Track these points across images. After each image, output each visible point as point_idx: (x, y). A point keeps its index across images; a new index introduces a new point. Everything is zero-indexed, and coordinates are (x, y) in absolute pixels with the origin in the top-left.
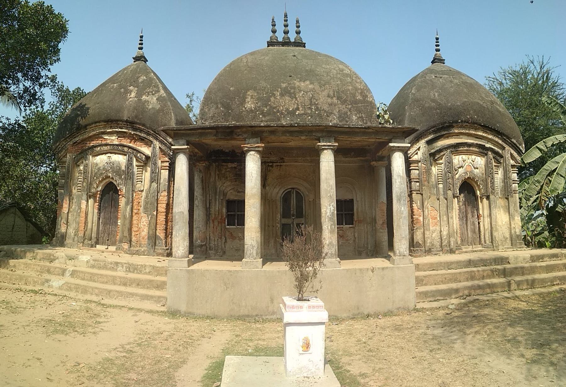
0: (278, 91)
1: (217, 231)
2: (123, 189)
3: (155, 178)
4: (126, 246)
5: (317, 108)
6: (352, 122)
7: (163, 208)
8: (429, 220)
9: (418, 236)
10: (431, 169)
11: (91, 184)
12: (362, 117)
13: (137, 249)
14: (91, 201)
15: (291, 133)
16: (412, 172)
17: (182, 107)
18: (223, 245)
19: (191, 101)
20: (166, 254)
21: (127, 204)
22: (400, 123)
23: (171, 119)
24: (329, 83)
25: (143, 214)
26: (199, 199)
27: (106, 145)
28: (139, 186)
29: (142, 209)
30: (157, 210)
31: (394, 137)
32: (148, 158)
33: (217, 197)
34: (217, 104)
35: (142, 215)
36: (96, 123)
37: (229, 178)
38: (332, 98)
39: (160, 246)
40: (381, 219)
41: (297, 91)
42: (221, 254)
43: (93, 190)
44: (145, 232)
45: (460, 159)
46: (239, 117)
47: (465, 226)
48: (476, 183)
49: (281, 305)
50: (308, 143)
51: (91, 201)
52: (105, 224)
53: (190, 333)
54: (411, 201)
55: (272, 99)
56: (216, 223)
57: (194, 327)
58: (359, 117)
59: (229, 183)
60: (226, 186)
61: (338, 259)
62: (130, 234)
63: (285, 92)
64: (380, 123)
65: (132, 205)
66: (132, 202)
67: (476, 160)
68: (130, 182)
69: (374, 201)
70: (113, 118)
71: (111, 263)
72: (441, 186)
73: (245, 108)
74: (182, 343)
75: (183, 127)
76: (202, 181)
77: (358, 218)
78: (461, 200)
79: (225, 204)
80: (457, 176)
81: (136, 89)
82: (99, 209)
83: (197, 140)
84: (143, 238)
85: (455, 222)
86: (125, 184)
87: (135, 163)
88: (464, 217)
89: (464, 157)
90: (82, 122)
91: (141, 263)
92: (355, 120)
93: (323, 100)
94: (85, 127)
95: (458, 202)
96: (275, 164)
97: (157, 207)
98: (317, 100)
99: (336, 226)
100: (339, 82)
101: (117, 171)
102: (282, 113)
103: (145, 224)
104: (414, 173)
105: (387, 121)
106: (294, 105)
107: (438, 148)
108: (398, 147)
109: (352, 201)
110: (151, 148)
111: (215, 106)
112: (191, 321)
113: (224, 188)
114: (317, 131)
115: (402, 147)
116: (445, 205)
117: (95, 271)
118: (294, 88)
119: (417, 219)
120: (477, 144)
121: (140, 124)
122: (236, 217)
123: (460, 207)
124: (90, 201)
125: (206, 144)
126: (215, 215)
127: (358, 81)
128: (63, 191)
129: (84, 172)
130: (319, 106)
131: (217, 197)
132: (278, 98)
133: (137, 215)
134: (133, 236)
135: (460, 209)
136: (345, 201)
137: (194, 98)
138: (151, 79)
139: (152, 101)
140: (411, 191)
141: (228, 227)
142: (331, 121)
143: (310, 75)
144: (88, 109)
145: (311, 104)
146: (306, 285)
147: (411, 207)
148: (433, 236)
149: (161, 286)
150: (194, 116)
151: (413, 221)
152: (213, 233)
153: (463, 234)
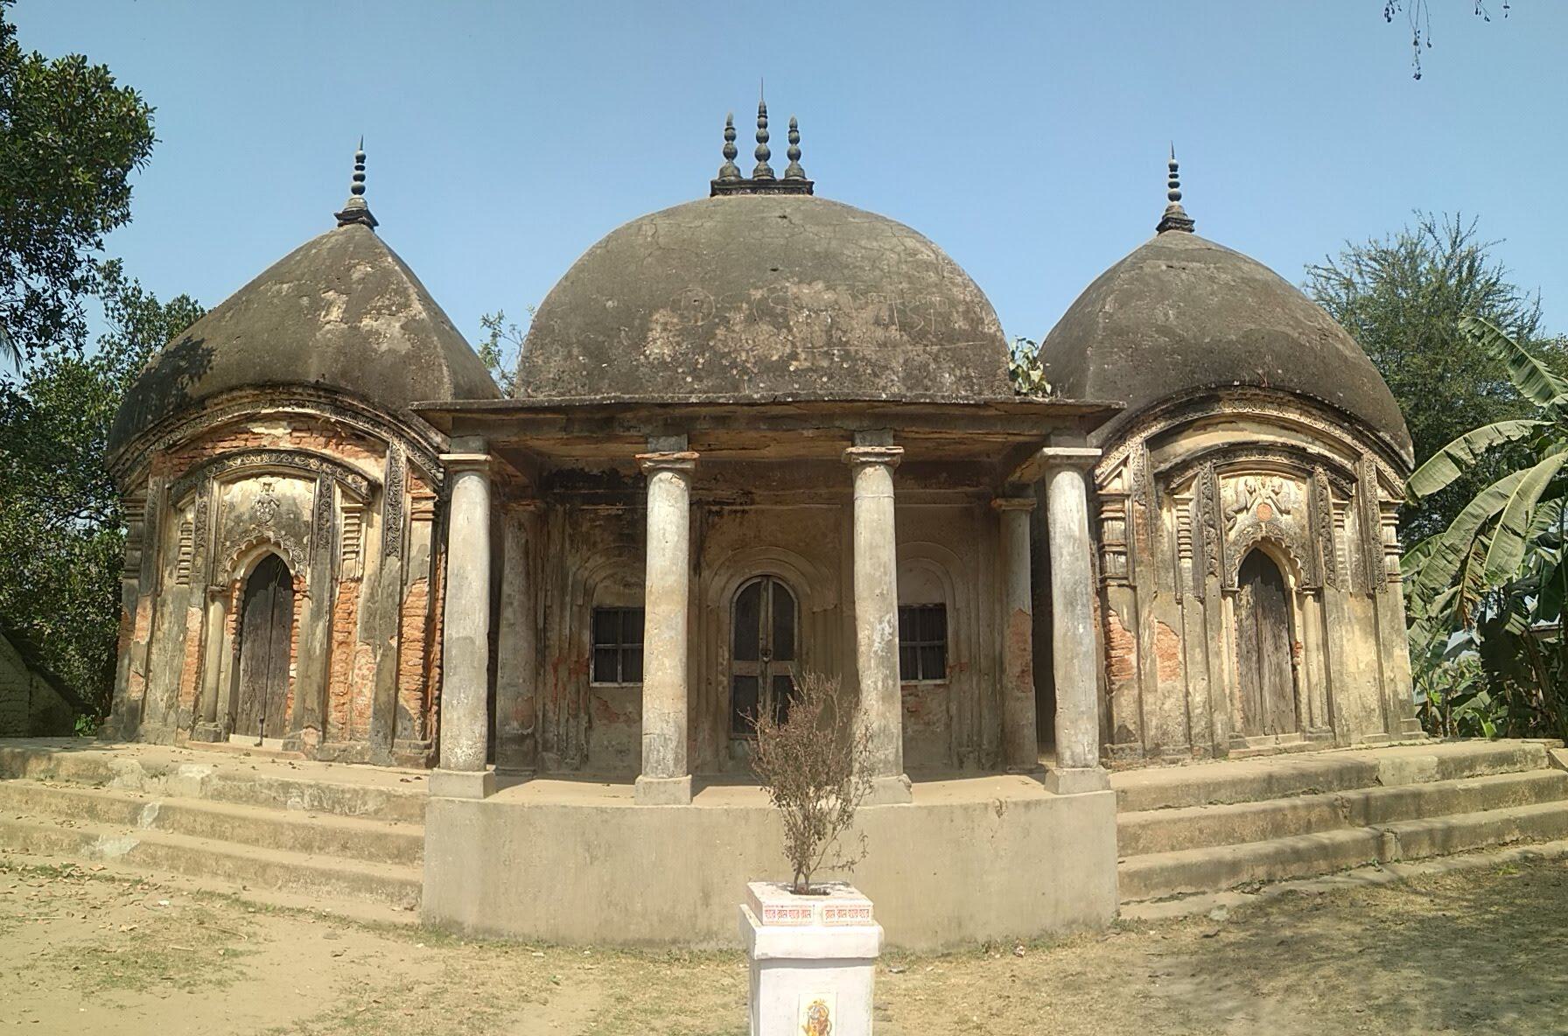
1: (562, 695)
2: (305, 575)
3: (396, 544)
4: (311, 737)
5: (847, 352)
6: (940, 389)
7: (417, 628)
8: (1153, 661)
9: (1125, 710)
10: (1158, 517)
11: (216, 561)
12: (968, 377)
14: (215, 609)
15: (775, 421)
16: (1108, 525)
17: (470, 349)
18: (583, 737)
19: (494, 336)
20: (422, 761)
21: (316, 615)
22: (1070, 392)
23: (441, 382)
24: (877, 287)
25: (359, 646)
26: (516, 604)
27: (260, 451)
28: (349, 565)
29: (357, 630)
30: (400, 635)
31: (1055, 428)
32: (375, 487)
33: (568, 599)
34: (568, 345)
35: (358, 648)
36: (231, 389)
37: (600, 546)
38: (886, 327)
39: (406, 737)
40: (1018, 657)
41: (793, 308)
42: (576, 761)
43: (222, 578)
44: (365, 697)
45: (1241, 487)
46: (631, 378)
47: (1256, 677)
48: (1286, 552)
49: (745, 907)
50: (822, 449)
51: (215, 609)
52: (254, 675)
53: (490, 988)
54: (1105, 608)
56: (563, 674)
57: (500, 971)
58: (961, 378)
59: (600, 560)
60: (591, 569)
61: (905, 777)
62: (324, 704)
64: (1018, 393)
65: (331, 621)
66: (331, 612)
67: (1285, 489)
68: (324, 554)
69: (997, 607)
70: (279, 377)
71: (270, 786)
72: (1187, 564)
73: (647, 357)
74: (468, 1015)
75: (474, 403)
76: (526, 553)
77: (959, 657)
78: (1244, 602)
79: (588, 619)
80: (1232, 535)
81: (344, 298)
82: (239, 632)
83: (514, 439)
85: (1225, 667)
86: (313, 561)
87: (339, 502)
88: (1252, 652)
89: (1251, 480)
90: (193, 389)
91: (352, 786)
92: (949, 385)
93: (862, 331)
94: (201, 402)
95: (1237, 607)
96: (727, 508)
97: (400, 626)
98: (845, 332)
99: (899, 683)
100: (905, 285)
101: (291, 524)
102: (745, 371)
104: (1113, 530)
105: (1037, 388)
106: (784, 345)
107: (1179, 460)
108: (1069, 457)
110: (384, 462)
111: (563, 352)
112: (493, 954)
113: (586, 574)
114: (845, 415)
115: (1080, 457)
116: (1199, 618)
117: (225, 807)
118: (785, 302)
119: (1122, 660)
120: (1284, 445)
121: (353, 395)
122: (620, 657)
123: (1240, 622)
124: (212, 609)
125: (540, 454)
126: (561, 649)
129: (198, 529)
130: (852, 349)
131: (568, 599)
132: (737, 328)
133: (344, 648)
134: (331, 709)
135: (1240, 629)
136: (924, 609)
137: (505, 327)
138: (387, 274)
139: (388, 332)
140: (1103, 580)
141: (596, 685)
142: (884, 389)
143: (824, 266)
144: (210, 352)
145: (829, 343)
146: (819, 849)
147: (1106, 625)
148: (1166, 707)
149: (408, 852)
150: (504, 376)
151: (1109, 666)
152: (555, 700)
153: (1248, 701)
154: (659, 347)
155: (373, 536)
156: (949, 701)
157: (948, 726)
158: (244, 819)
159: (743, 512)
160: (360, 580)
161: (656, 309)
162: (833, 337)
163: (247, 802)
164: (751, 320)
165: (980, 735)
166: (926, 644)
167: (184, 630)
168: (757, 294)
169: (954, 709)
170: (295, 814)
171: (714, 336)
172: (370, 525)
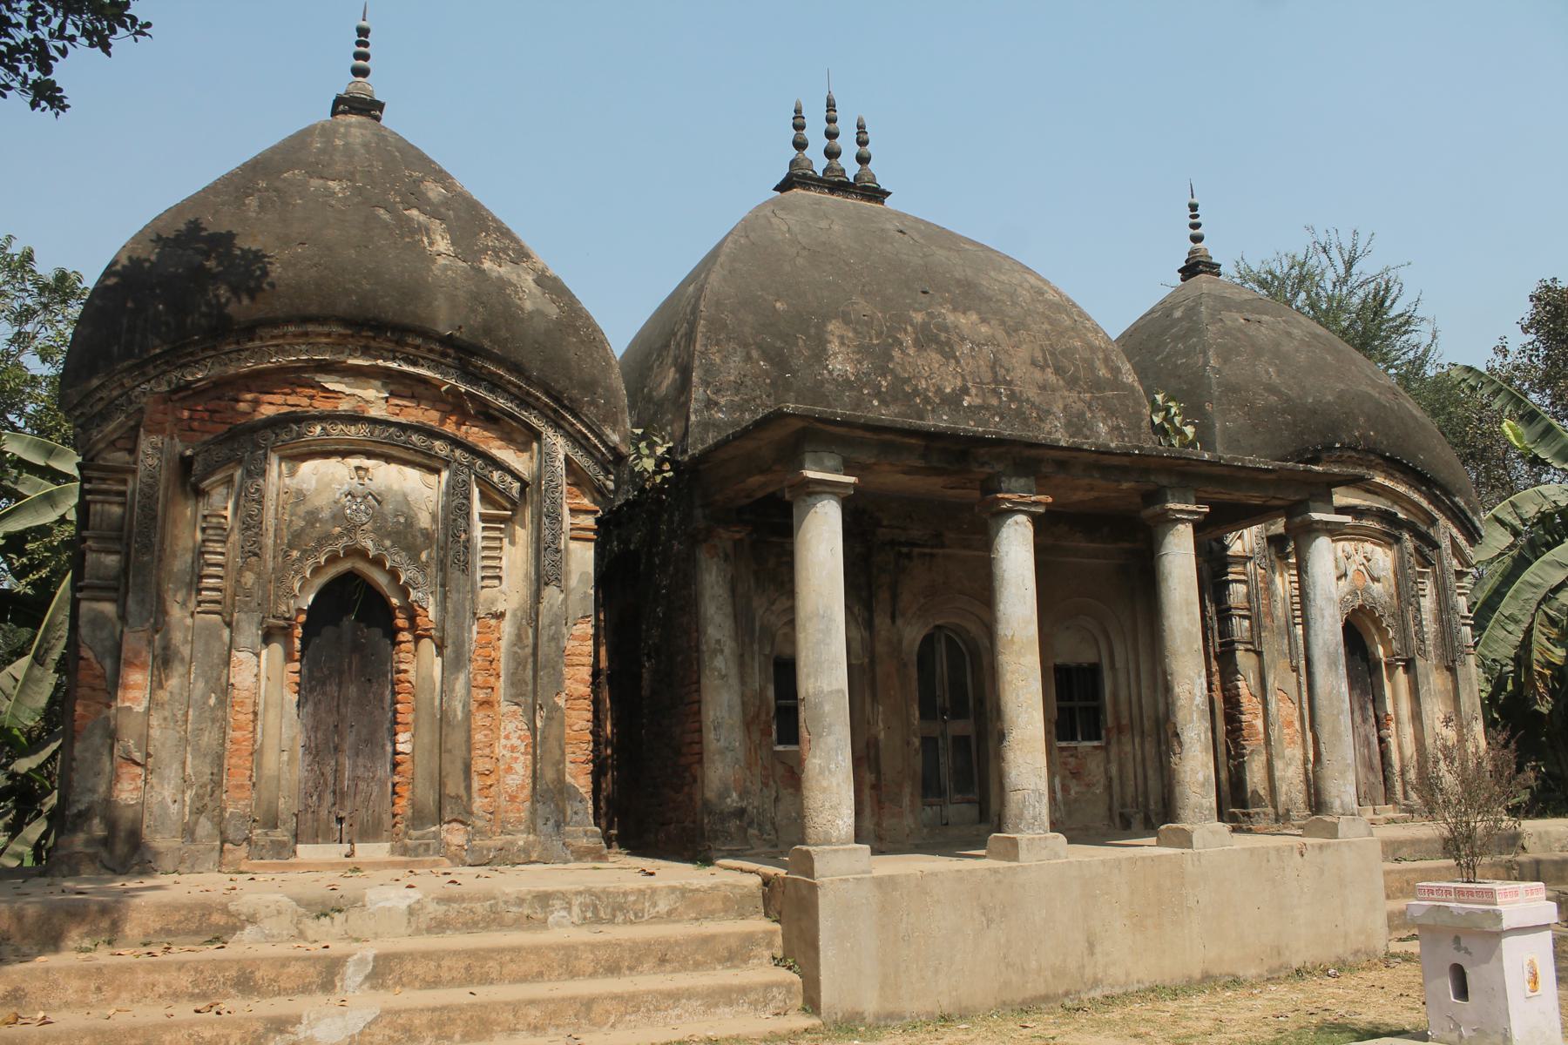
0: (905, 331)
5: (1013, 392)
7: (582, 681)
10: (1272, 581)
12: (1118, 428)
13: (499, 840)
25: (505, 707)
26: (727, 651)
29: (501, 685)
34: (746, 345)
38: (1043, 369)
39: (578, 824)
44: (518, 776)
46: (816, 392)
55: (896, 353)
63: (929, 338)
73: (830, 373)
77: (1117, 717)
84: (512, 799)
96: (916, 550)
98: (1008, 370)
100: (1046, 326)
102: (927, 400)
103: (515, 741)
104: (1237, 592)
106: (954, 377)
109: (1094, 671)
111: (741, 353)
118: (946, 329)
124: (264, 653)
127: (1088, 325)
128: (109, 608)
131: (756, 647)
132: (911, 352)
134: (475, 795)
141: (780, 748)
145: (995, 381)
154: (840, 363)
155: (515, 557)
156: (1108, 761)
157: (1109, 787)
158: (517, 950)
159: (932, 555)
160: (500, 616)
161: (826, 318)
162: (998, 376)
163: (487, 928)
164: (920, 345)
165: (1146, 798)
166: (1082, 704)
167: (225, 690)
168: (918, 318)
169: (1114, 770)
170: (563, 930)
171: (891, 358)
172: (512, 543)
